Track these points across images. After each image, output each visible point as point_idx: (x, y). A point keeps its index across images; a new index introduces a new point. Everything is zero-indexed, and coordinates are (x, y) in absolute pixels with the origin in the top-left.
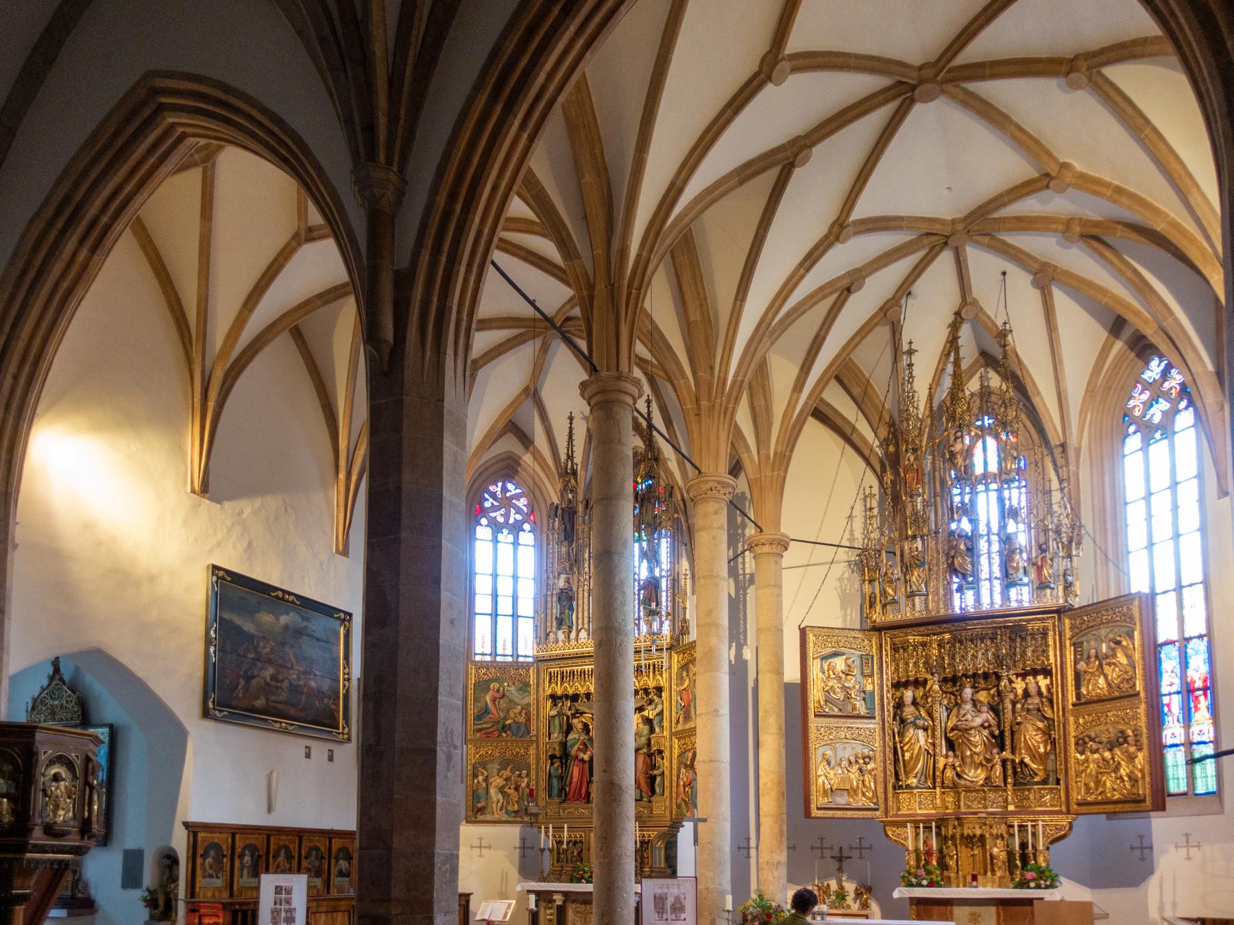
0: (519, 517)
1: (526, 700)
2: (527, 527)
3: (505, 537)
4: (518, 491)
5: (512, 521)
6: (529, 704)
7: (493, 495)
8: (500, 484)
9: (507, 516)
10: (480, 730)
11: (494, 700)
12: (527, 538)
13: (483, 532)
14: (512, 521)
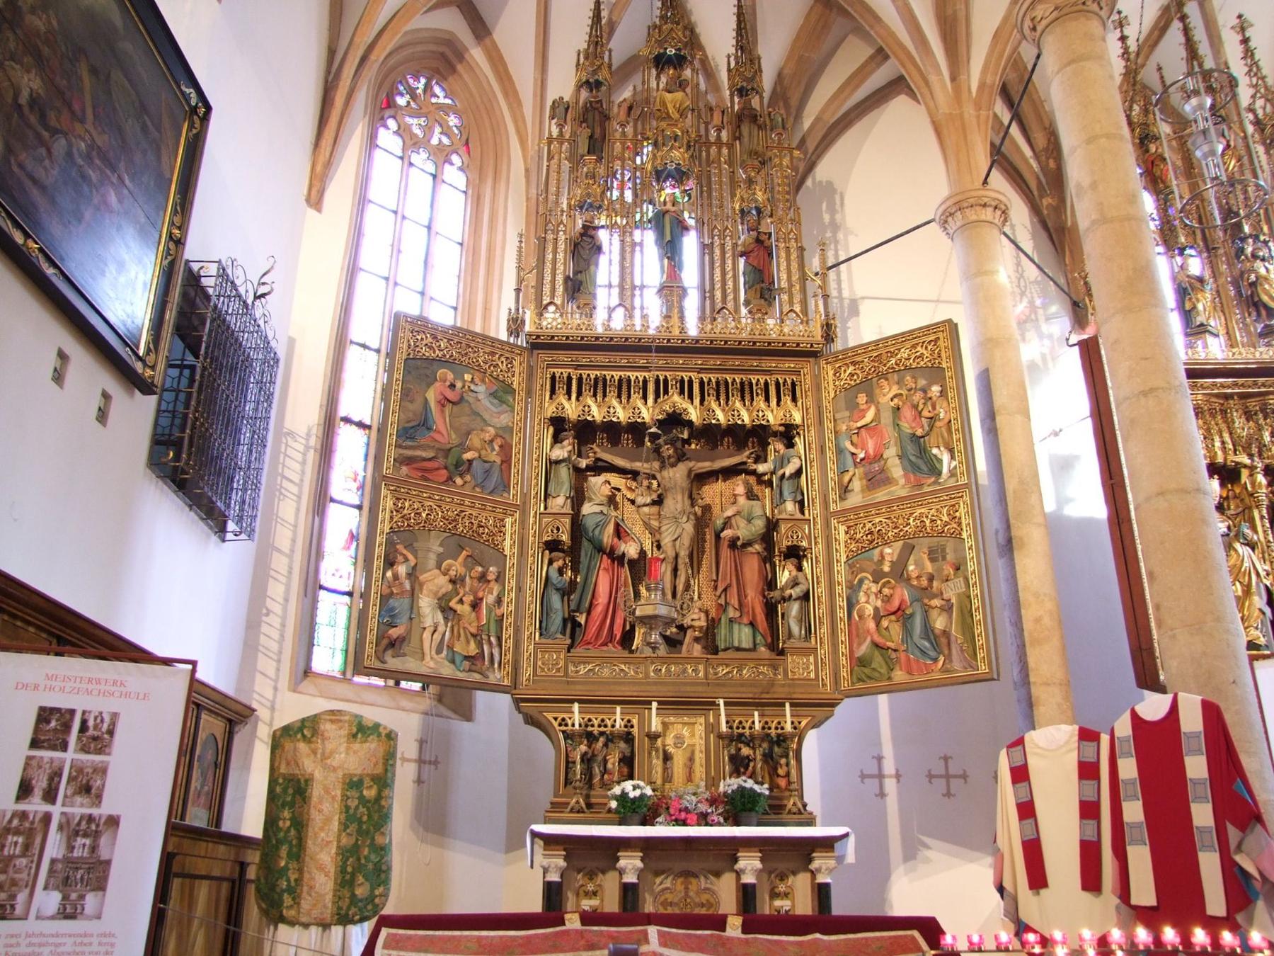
0: (446, 141)
1: (504, 420)
2: (455, 158)
3: (419, 158)
4: (448, 101)
5: (435, 141)
6: (510, 430)
7: (412, 92)
8: (423, 81)
9: (428, 130)
10: (408, 461)
11: (444, 402)
12: (454, 175)
13: (388, 138)
14: (435, 141)
